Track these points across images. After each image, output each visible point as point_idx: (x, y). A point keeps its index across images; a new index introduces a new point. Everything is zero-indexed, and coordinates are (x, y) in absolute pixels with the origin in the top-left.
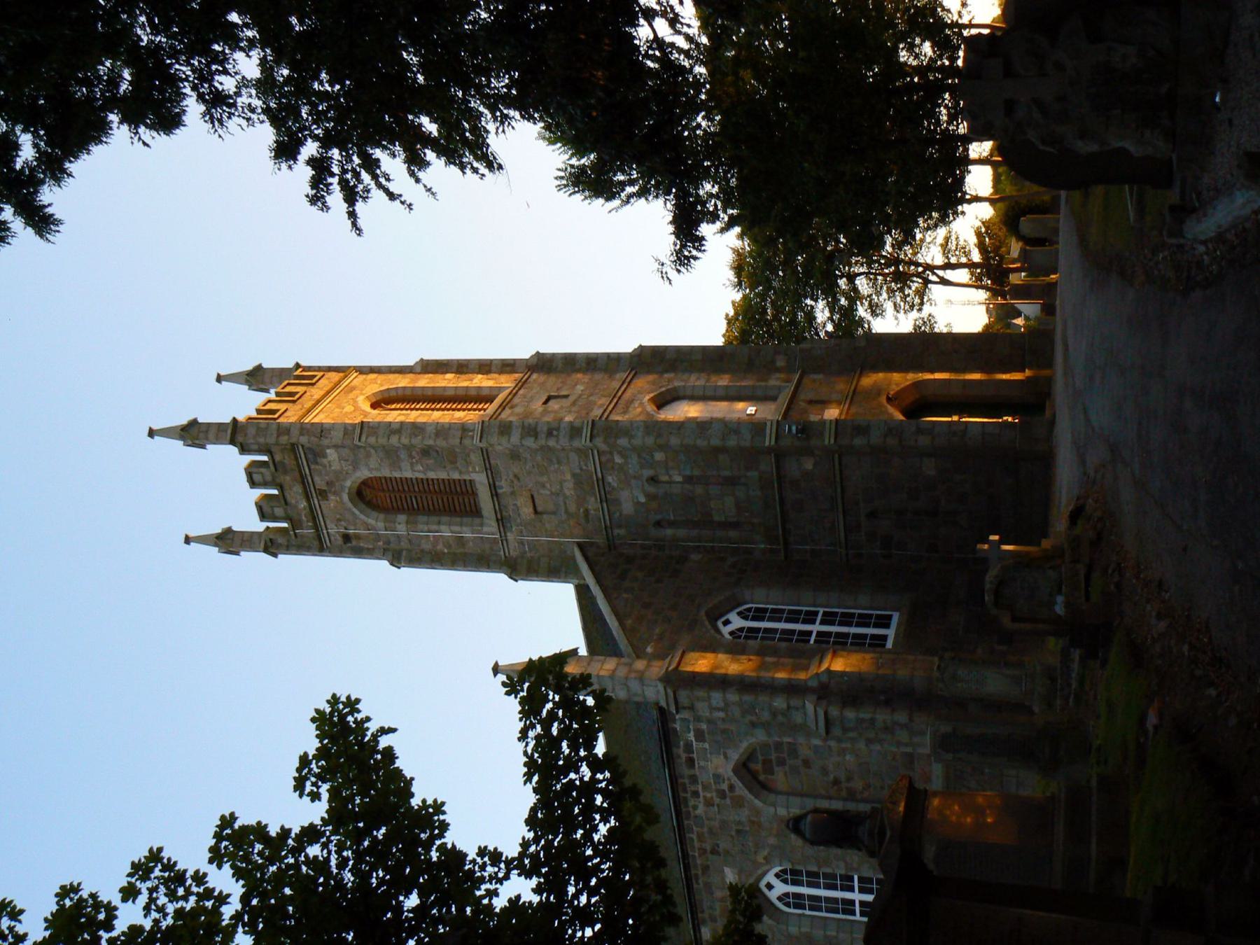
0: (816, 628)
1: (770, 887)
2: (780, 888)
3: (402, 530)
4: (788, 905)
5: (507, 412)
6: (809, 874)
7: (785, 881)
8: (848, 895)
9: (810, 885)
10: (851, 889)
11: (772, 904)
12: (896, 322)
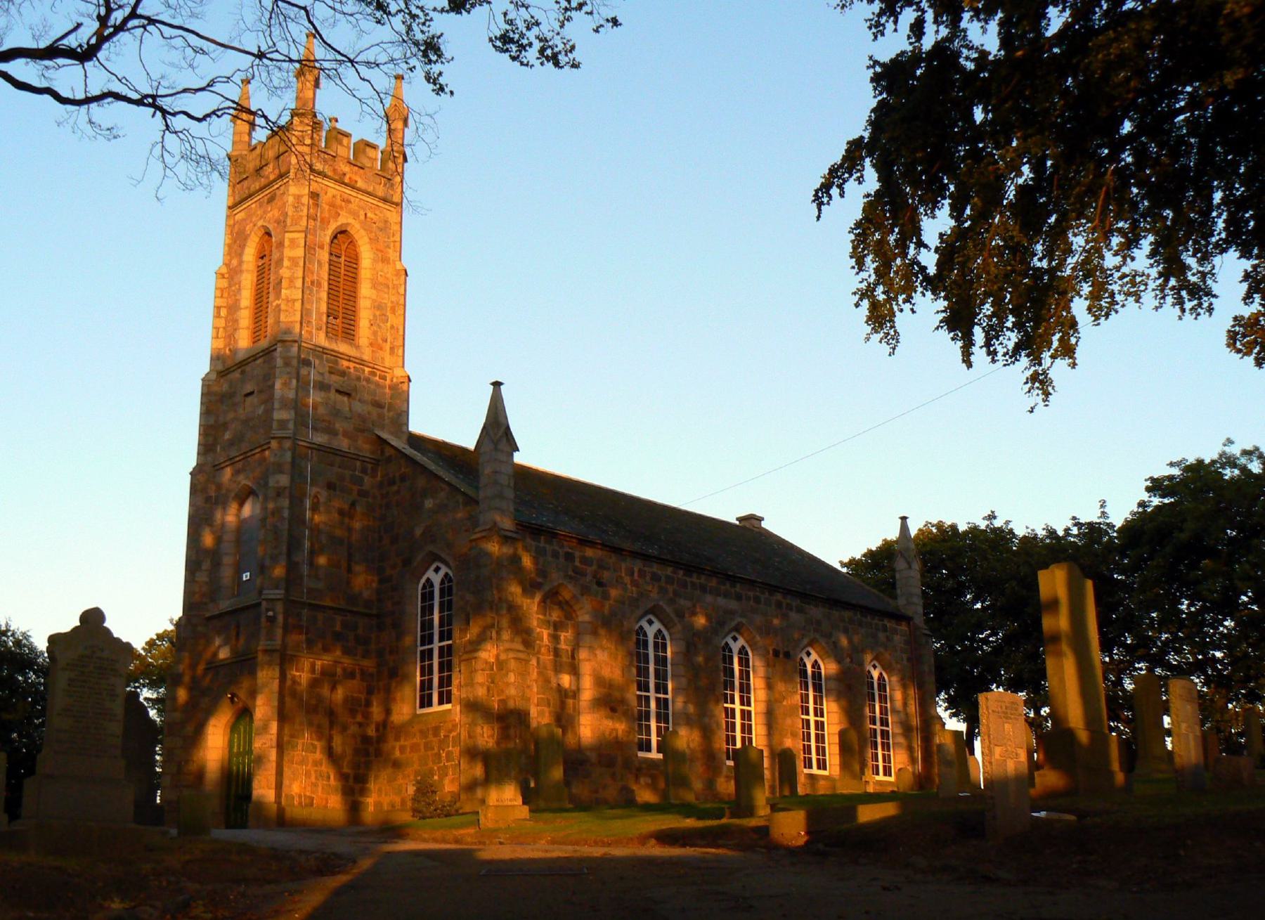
1: (437, 570)
2: (436, 579)
4: (424, 587)
6: (450, 602)
7: (442, 582)
8: (436, 637)
10: (441, 640)
11: (424, 574)
12: (439, 9)
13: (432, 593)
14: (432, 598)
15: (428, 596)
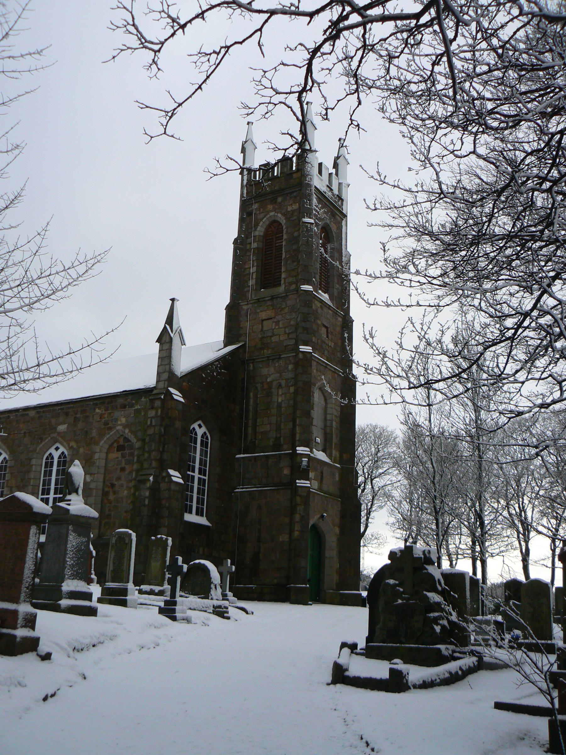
0: (196, 475)
1: (57, 449)
2: (56, 455)
3: (254, 245)
4: (47, 458)
5: (319, 305)
7: (60, 457)
8: (52, 491)
9: (58, 471)
10: (55, 493)
13: (52, 463)
14: (52, 465)
15: (49, 464)
